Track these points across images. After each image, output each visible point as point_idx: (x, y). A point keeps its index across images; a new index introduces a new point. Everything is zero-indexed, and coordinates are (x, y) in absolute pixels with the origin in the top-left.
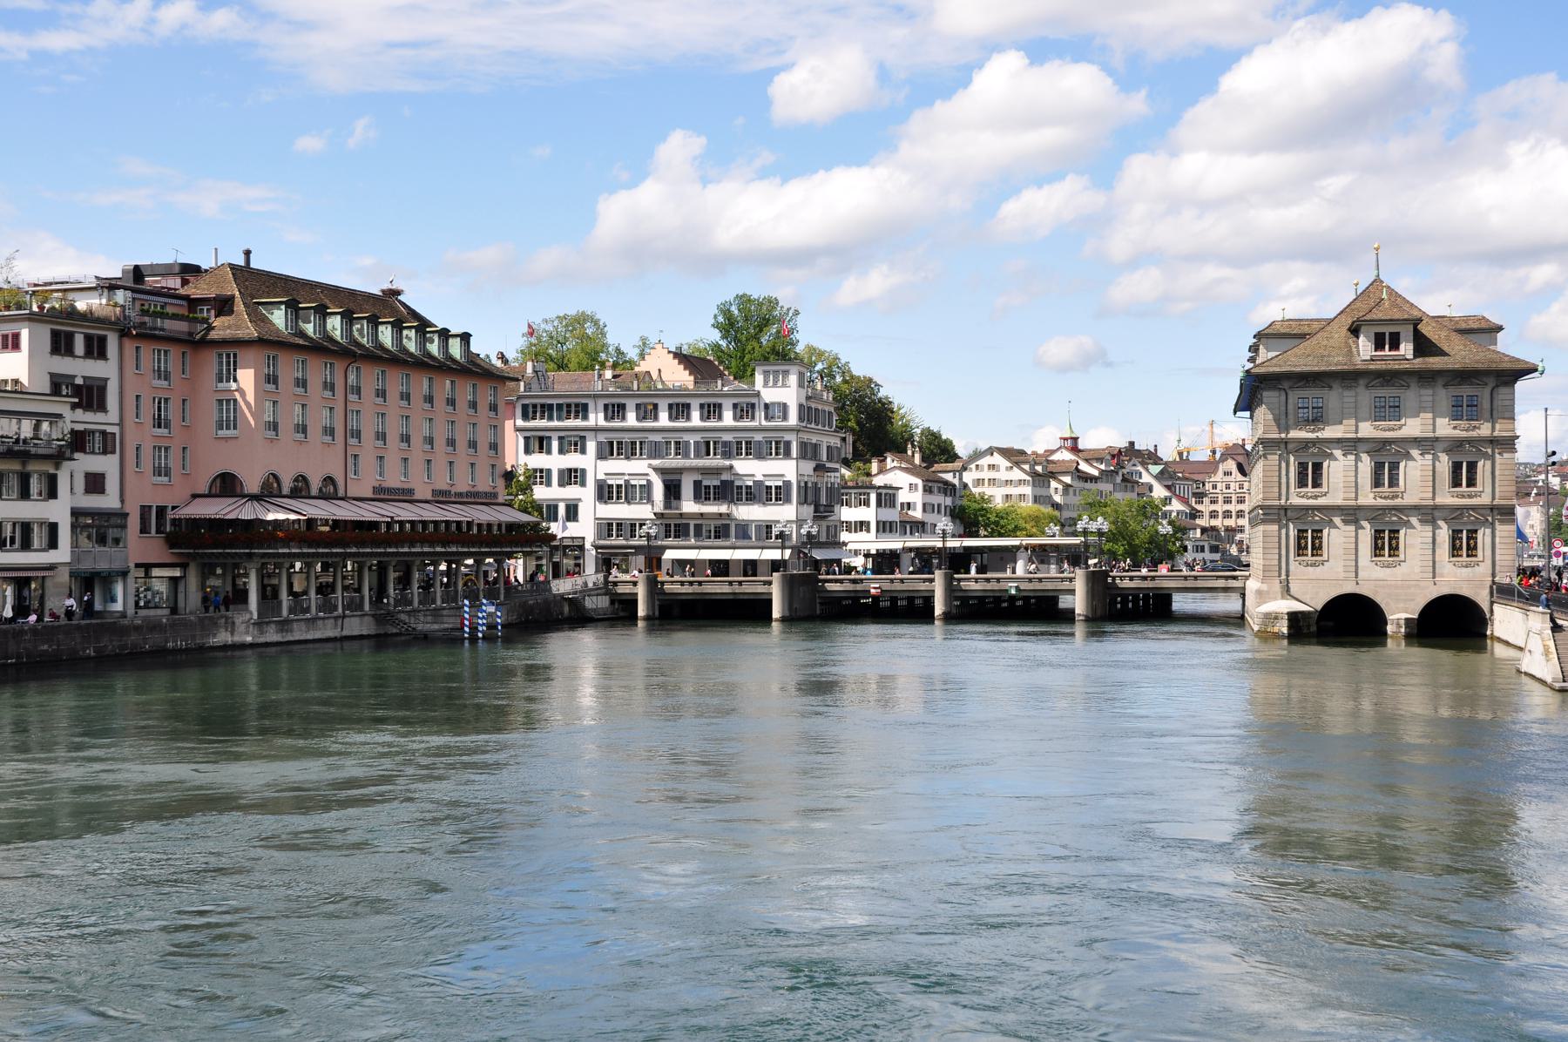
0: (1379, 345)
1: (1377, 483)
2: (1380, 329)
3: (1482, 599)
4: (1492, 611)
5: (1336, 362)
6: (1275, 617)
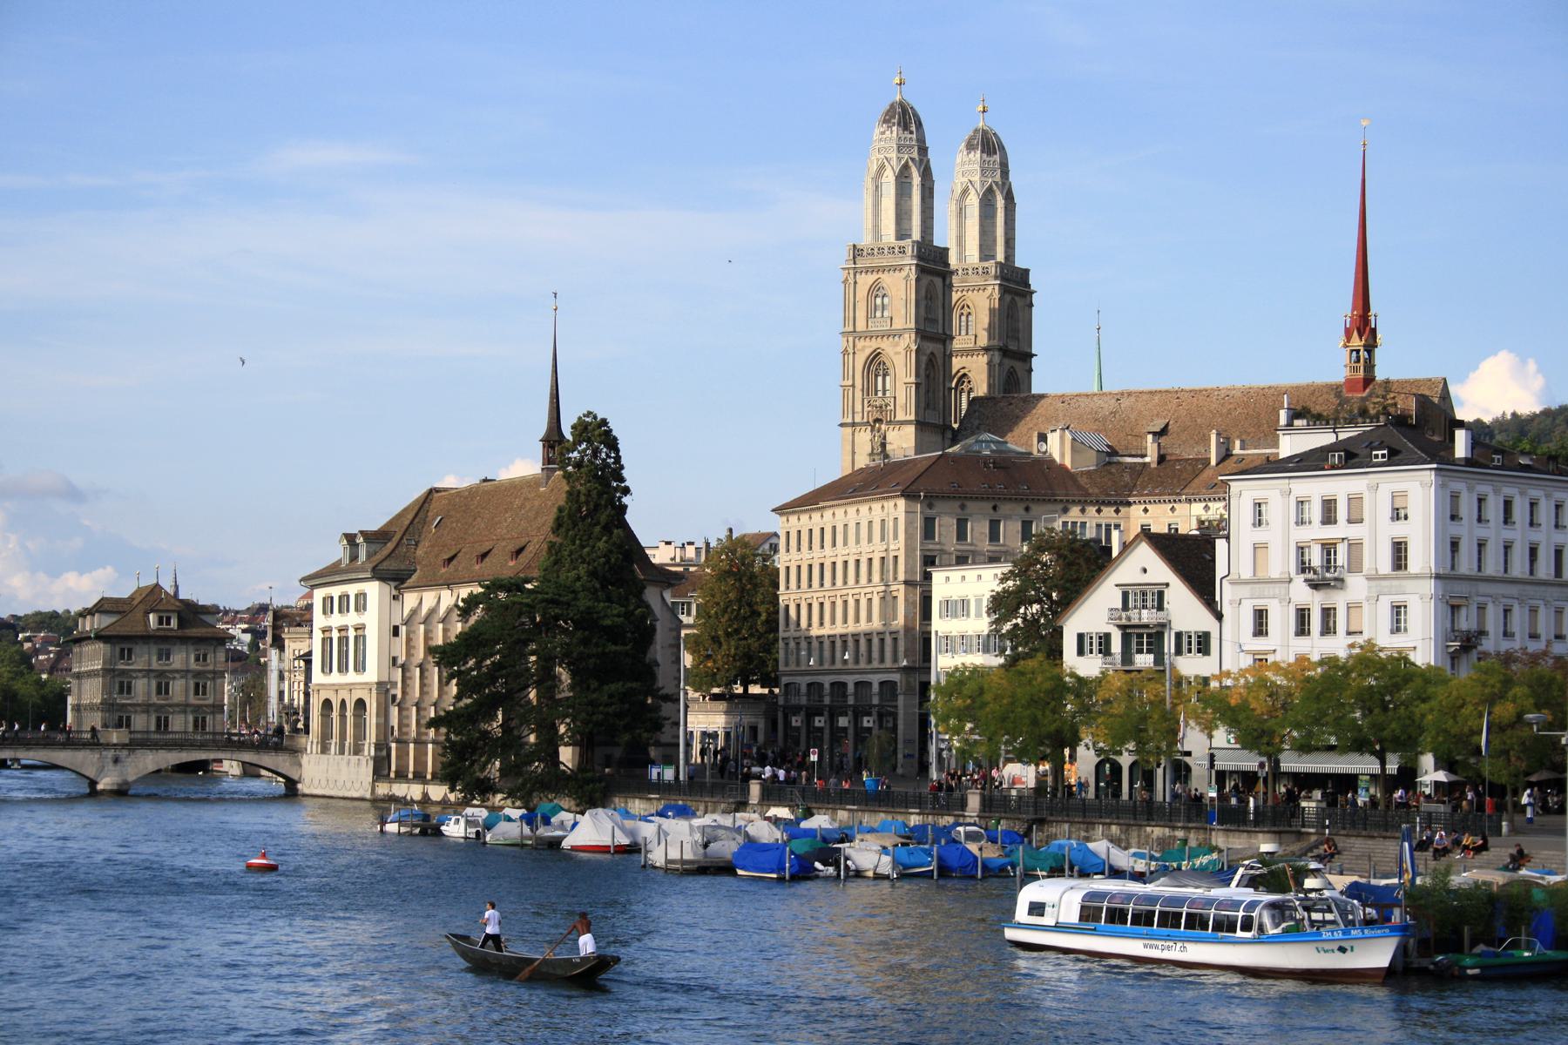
0: (161, 623)
1: (159, 692)
5: (138, 630)
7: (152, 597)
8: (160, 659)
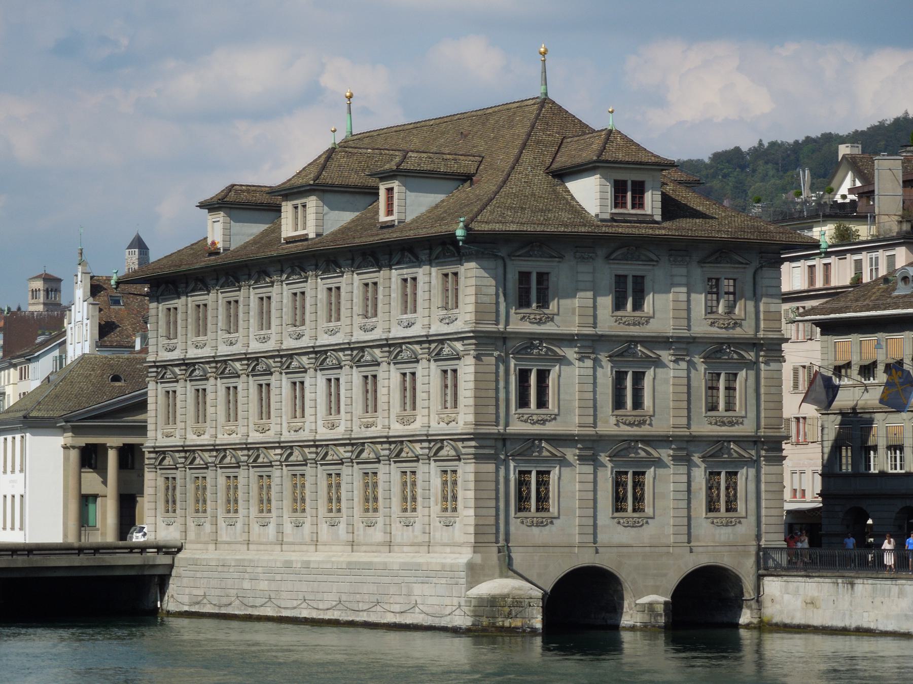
0: (619, 201)
1: (619, 403)
2: (621, 176)
3: (746, 569)
4: (758, 588)
6: (518, 603)
7: (551, 136)
8: (619, 305)
